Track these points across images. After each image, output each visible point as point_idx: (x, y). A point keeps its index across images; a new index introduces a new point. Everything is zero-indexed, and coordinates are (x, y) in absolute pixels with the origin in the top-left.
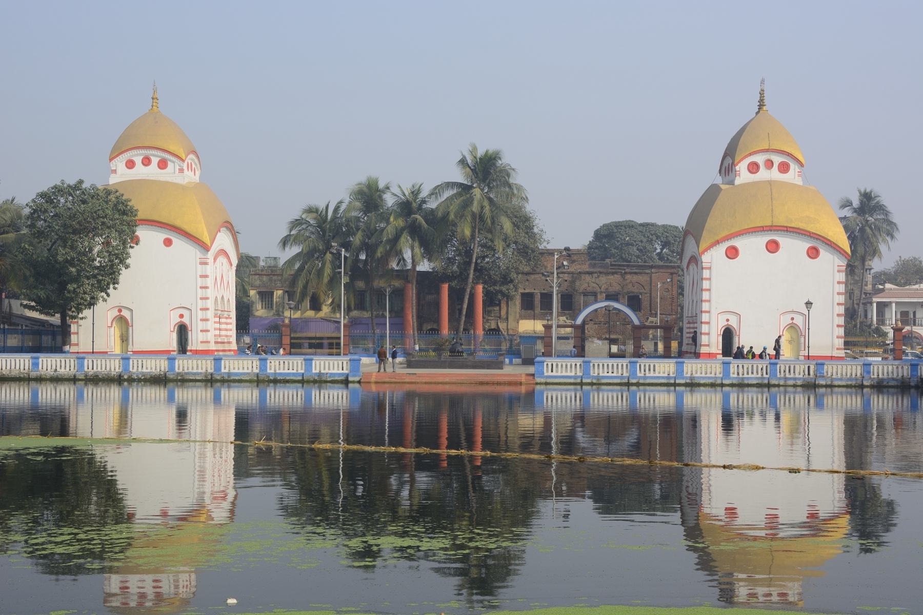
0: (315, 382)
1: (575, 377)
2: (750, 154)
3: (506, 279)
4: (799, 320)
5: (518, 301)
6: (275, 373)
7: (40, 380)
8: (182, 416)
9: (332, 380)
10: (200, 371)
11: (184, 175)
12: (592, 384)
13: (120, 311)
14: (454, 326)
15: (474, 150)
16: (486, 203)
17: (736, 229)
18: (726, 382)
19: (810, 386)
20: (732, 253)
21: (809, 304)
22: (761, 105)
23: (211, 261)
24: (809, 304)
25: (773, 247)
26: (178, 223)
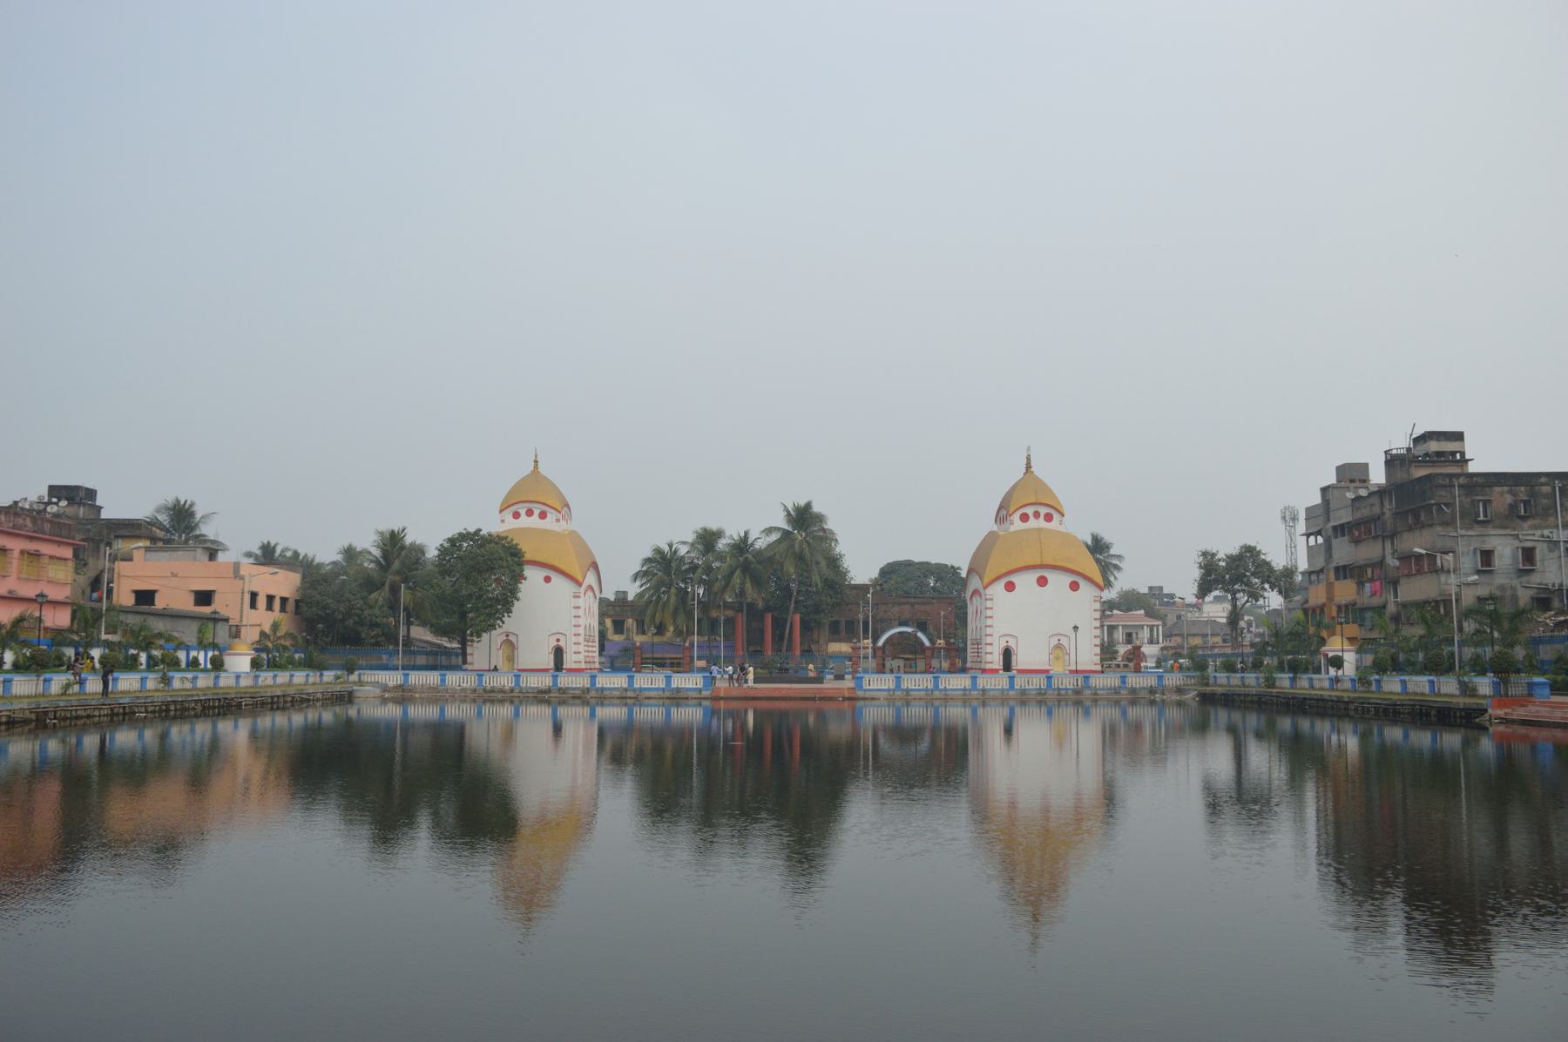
4: (1064, 642)
9: (687, 693)
14: (777, 650)
20: (1010, 587)
21: (1076, 628)
22: (1028, 466)
24: (1076, 628)
25: (1042, 581)
26: (556, 563)
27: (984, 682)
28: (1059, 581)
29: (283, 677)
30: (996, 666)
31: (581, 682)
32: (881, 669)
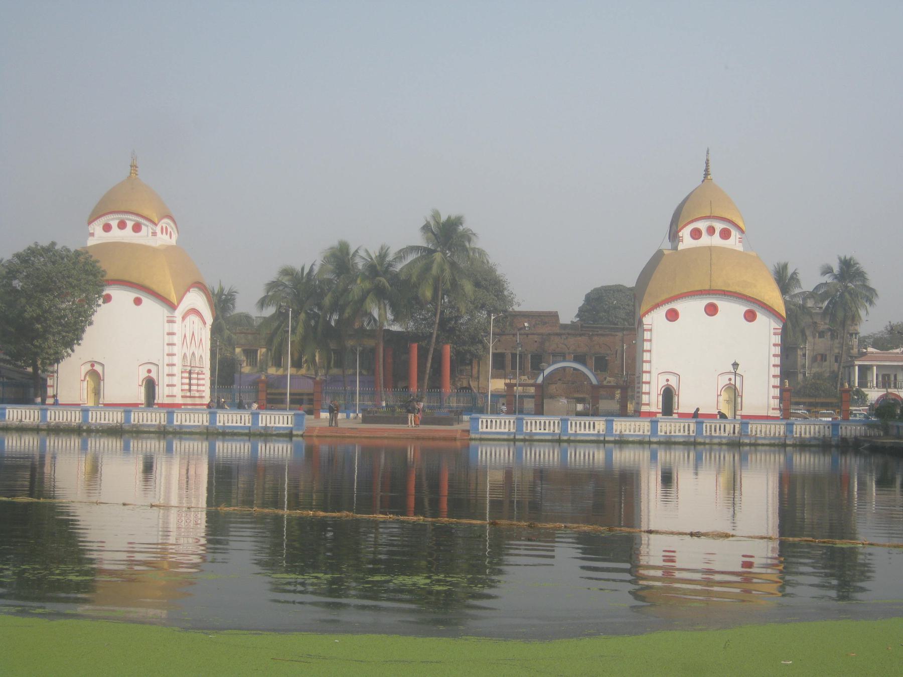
0: (261, 435)
1: (509, 433)
2: (692, 221)
3: (475, 340)
6: (224, 427)
8: (148, 468)
9: (275, 433)
10: (154, 423)
11: (159, 237)
12: (524, 440)
13: (93, 365)
16: (447, 267)
17: (676, 293)
18: (654, 439)
19: (734, 445)
20: (673, 315)
21: (735, 365)
22: (707, 173)
23: (179, 319)
25: (712, 310)
28: (733, 311)
30: (653, 409)
32: (539, 411)
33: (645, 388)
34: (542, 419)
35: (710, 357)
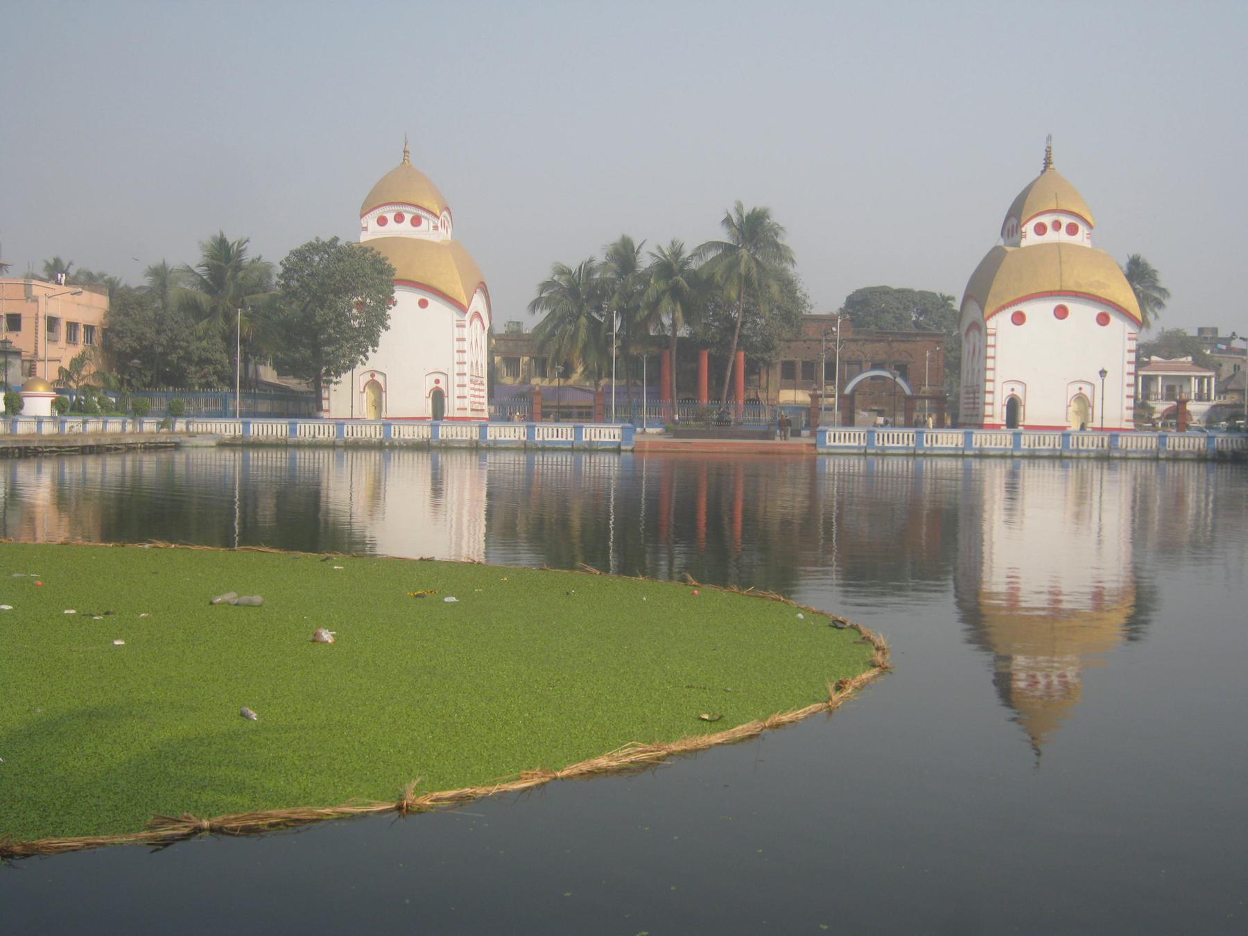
1: (859, 448)
2: (1038, 215)
4: (1087, 390)
5: (779, 369)
6: (543, 441)
7: (299, 446)
9: (604, 446)
11: (432, 232)
12: (876, 455)
13: (373, 375)
14: (716, 396)
15: (739, 208)
16: (753, 264)
17: (1022, 294)
18: (1017, 453)
20: (1019, 319)
21: (1103, 373)
22: (1048, 162)
23: (467, 324)
24: (1103, 373)
27: (980, 439)
28: (1084, 313)
29: (93, 426)
31: (468, 433)
32: (849, 421)
33: (988, 398)
34: (851, 430)
35: (1054, 364)
